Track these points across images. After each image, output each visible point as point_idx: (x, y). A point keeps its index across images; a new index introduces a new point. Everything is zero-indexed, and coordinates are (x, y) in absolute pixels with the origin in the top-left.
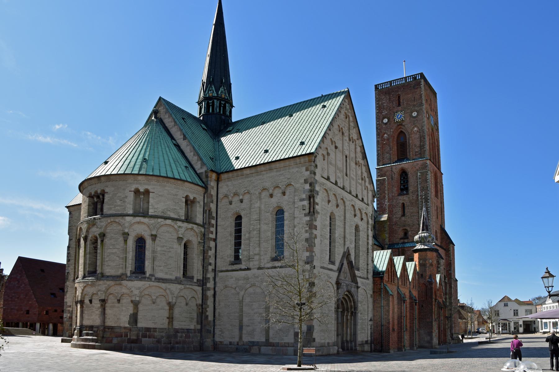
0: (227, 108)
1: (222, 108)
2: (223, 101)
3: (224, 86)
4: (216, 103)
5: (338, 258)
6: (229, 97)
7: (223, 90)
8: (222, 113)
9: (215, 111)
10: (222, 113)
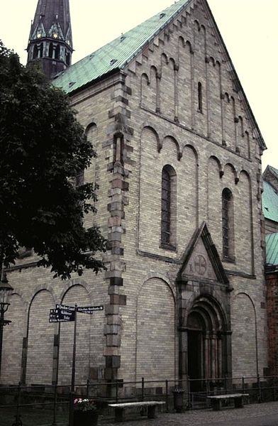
0: (61, 51)
1: (54, 52)
2: (56, 42)
3: (57, 24)
4: (46, 46)
5: (182, 244)
6: (65, 35)
7: (55, 28)
8: (53, 57)
9: (44, 56)
10: (53, 57)
